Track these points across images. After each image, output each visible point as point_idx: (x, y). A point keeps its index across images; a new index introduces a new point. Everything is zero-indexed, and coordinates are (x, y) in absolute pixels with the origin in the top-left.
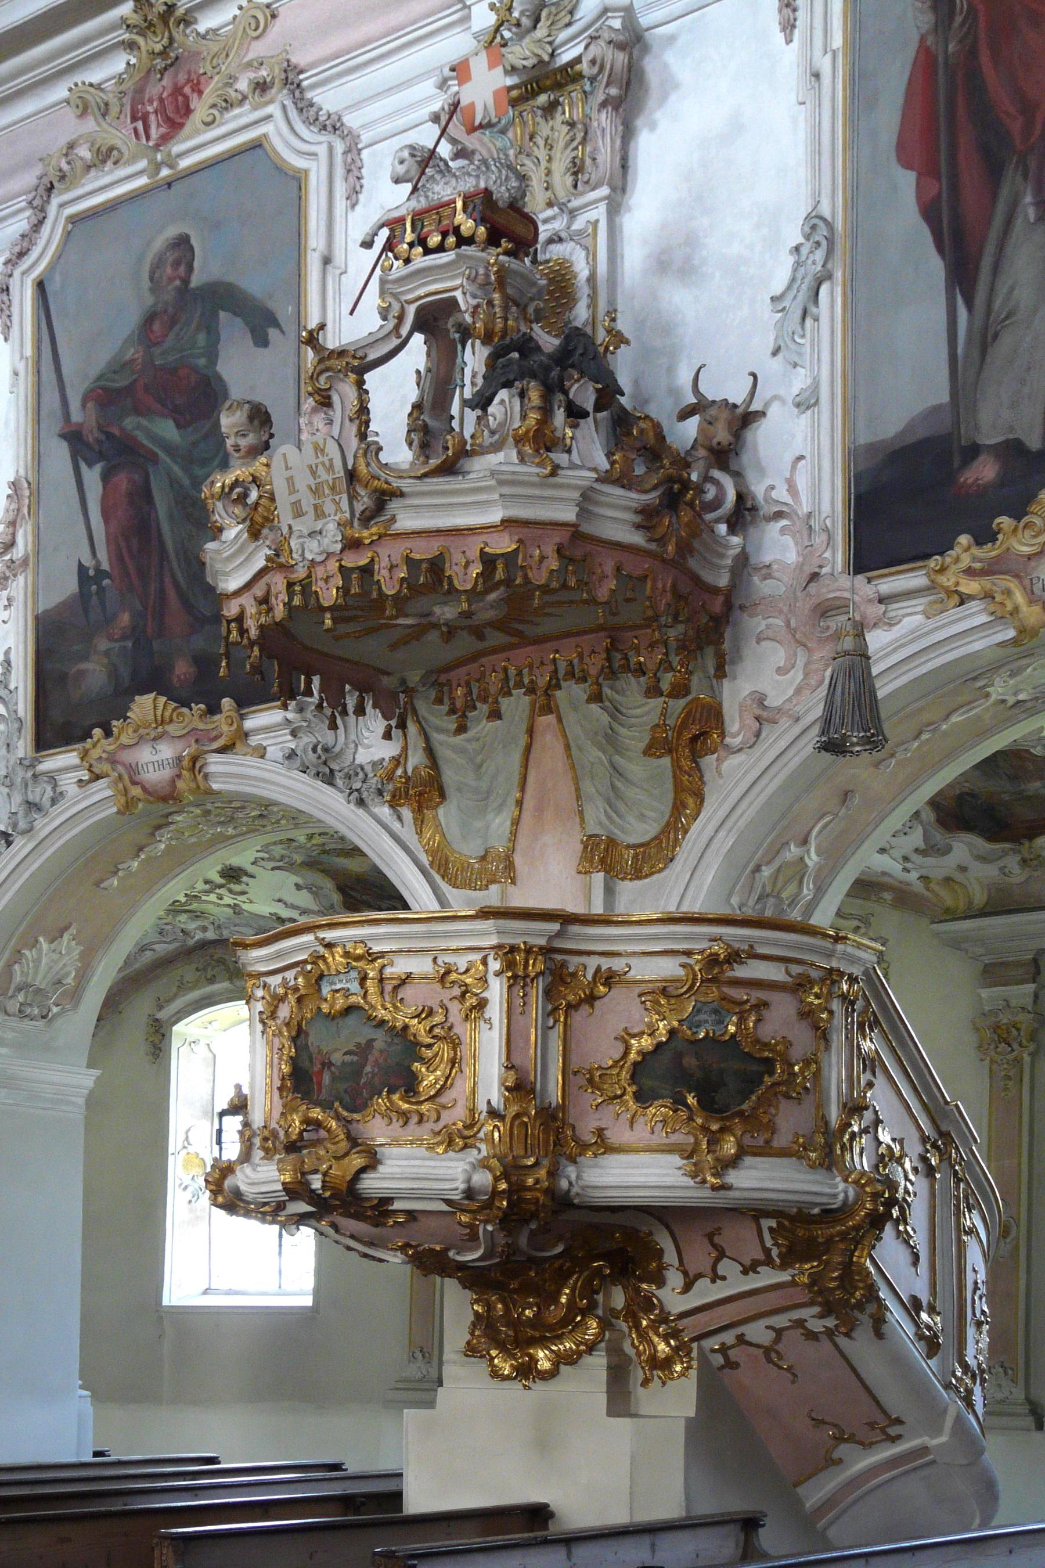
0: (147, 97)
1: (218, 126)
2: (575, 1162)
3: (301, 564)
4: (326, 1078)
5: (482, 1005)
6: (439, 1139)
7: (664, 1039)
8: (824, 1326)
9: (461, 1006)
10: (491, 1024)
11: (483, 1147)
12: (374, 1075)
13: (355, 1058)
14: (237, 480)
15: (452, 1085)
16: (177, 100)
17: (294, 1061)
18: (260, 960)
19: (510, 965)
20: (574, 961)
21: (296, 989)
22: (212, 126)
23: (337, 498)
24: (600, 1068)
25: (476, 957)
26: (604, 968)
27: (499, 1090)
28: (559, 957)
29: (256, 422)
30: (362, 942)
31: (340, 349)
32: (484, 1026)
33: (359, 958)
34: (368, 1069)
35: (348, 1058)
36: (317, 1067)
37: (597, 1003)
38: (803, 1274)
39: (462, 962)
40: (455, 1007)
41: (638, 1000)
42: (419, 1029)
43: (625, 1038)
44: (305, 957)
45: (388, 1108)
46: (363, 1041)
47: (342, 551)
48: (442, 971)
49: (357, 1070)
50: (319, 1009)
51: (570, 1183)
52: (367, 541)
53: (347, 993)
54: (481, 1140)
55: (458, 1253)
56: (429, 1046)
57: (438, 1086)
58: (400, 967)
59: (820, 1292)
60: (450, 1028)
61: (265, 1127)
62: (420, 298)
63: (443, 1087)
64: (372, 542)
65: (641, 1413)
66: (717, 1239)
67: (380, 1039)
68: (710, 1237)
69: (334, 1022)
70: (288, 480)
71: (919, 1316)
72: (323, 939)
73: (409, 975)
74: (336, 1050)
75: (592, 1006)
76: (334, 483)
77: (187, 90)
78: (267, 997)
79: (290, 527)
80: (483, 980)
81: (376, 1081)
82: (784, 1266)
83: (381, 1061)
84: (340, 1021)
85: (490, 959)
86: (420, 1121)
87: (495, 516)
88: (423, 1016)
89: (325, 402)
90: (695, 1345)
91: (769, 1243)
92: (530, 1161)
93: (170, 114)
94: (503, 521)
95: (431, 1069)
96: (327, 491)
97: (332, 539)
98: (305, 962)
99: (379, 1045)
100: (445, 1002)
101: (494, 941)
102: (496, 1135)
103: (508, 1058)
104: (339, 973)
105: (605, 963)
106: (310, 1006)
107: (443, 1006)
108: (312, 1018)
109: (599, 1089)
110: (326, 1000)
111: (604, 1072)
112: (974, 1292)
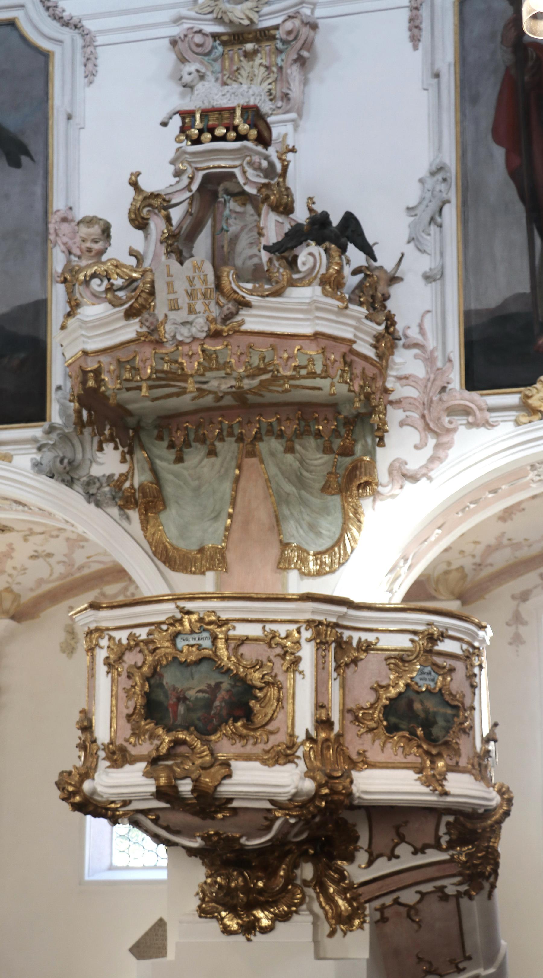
3: (171, 342)
4: (181, 709)
5: (297, 661)
7: (403, 691)
9: (282, 662)
10: (304, 675)
12: (221, 706)
13: (206, 695)
14: (95, 272)
15: (276, 717)
17: (147, 696)
19: (318, 634)
20: (346, 634)
24: (362, 708)
25: (293, 627)
26: (363, 639)
28: (340, 631)
30: (214, 612)
31: (156, 193)
32: (298, 677)
34: (217, 703)
35: (200, 695)
36: (172, 701)
37: (360, 664)
39: (282, 630)
40: (278, 661)
41: (384, 663)
42: (256, 677)
43: (377, 688)
45: (233, 733)
46: (213, 683)
47: (205, 338)
49: (208, 704)
52: (225, 334)
55: (247, 840)
56: (261, 689)
58: (242, 630)
60: (276, 676)
61: (111, 743)
62: (209, 168)
65: (329, 956)
66: (402, 830)
68: (397, 828)
69: (189, 669)
72: (183, 608)
74: (190, 689)
75: (356, 665)
79: (166, 316)
80: (298, 643)
81: (224, 712)
84: (194, 669)
85: (303, 630)
86: (255, 743)
87: (308, 330)
88: (258, 667)
90: (367, 905)
96: (199, 296)
100: (272, 658)
101: (309, 616)
105: (365, 636)
108: (167, 665)
109: (362, 723)
111: (366, 711)
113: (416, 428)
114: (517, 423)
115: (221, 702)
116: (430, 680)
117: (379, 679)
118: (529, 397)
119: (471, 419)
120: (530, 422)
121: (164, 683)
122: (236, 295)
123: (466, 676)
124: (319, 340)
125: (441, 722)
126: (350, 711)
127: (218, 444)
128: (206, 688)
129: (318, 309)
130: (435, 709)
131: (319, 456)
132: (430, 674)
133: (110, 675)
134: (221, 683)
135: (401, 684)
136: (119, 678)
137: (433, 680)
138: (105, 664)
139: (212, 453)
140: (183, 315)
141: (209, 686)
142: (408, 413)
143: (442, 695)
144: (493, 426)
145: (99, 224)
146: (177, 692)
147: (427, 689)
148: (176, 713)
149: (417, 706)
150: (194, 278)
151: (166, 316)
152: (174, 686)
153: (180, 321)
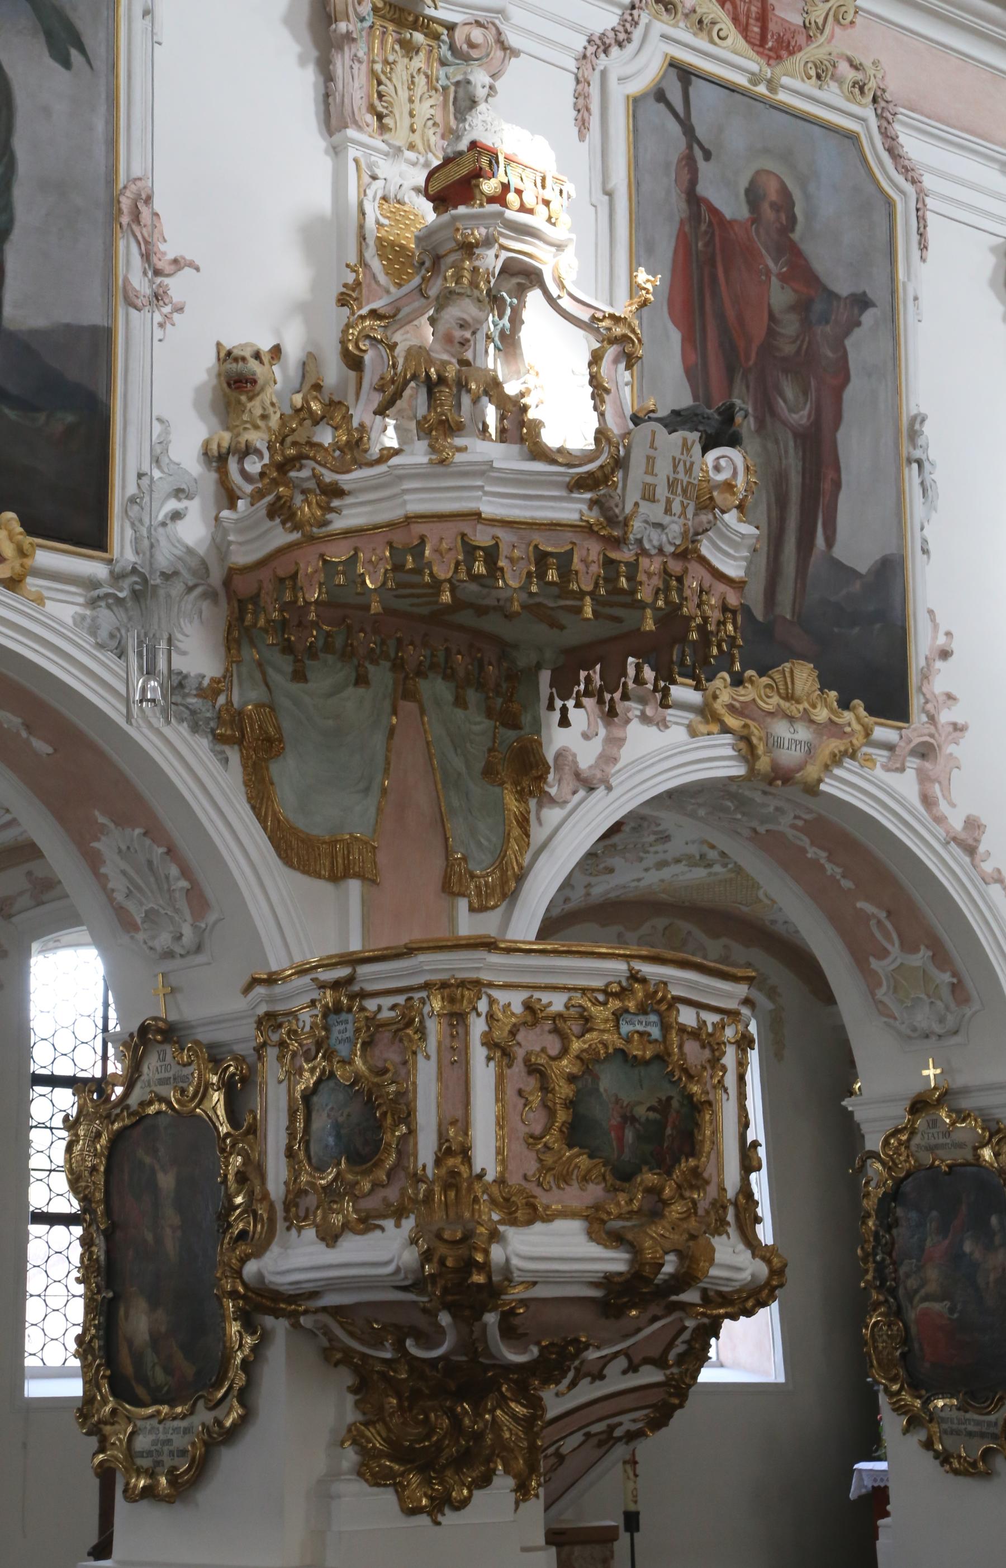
34: (669, 1131)
35: (652, 1115)
46: (664, 1098)
74: (640, 1103)
99: (675, 1104)
114: (693, 733)
121: (602, 1090)
127: (371, 668)
128: (656, 1104)
131: (478, 719)
133: (492, 1064)
136: (509, 1071)
138: (483, 1044)
139: (361, 680)
140: (655, 512)
141: (660, 1101)
146: (622, 1107)
148: (621, 1139)
151: (636, 504)
152: (616, 1096)
153: (653, 519)
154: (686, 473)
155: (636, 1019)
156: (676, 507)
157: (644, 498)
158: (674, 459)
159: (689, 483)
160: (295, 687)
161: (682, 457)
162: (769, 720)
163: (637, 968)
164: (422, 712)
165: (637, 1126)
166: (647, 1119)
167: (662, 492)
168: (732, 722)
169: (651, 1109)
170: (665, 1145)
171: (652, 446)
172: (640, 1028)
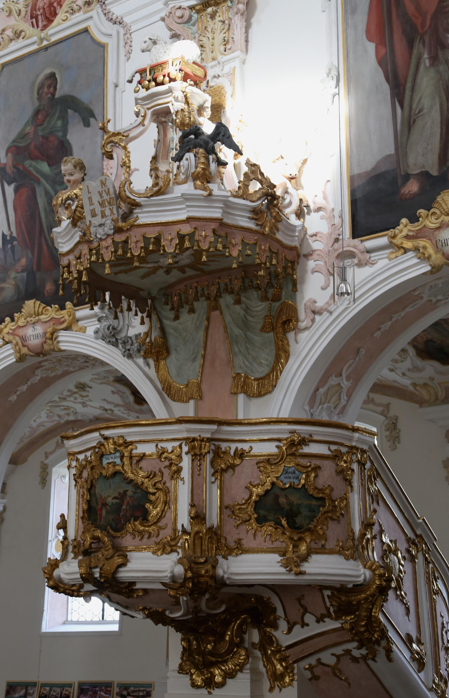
0: (37, 7)
1: (69, 21)
2: (227, 559)
6: (159, 546)
8: (361, 654)
11: (180, 551)
12: (126, 509)
16: (50, 9)
18: (73, 446)
21: (90, 462)
22: (66, 21)
23: (111, 207)
27: (188, 518)
29: (78, 168)
33: (120, 445)
38: (347, 623)
44: (95, 444)
48: (160, 453)
50: (101, 473)
51: (224, 572)
53: (114, 464)
54: (179, 547)
56: (154, 494)
57: (158, 517)
59: (356, 634)
60: (164, 484)
63: (160, 516)
64: (127, 229)
67: (130, 490)
70: (89, 198)
71: (412, 646)
73: (144, 455)
76: (110, 200)
77: (55, 4)
78: (78, 466)
82: (337, 618)
83: (130, 502)
87: (183, 217)
89: (111, 157)
91: (328, 604)
92: (202, 560)
93: (48, 16)
94: (187, 218)
95: (155, 506)
97: (108, 229)
98: (94, 447)
102: (186, 545)
103: (192, 500)
104: (111, 453)
106: (97, 472)
107: (160, 471)
110: (104, 468)
112: (442, 630)
113: (322, 273)
115: (127, 506)
116: (293, 478)
117: (252, 480)
118: (394, 237)
119: (356, 261)
120: (396, 257)
122: (129, 199)
123: (336, 471)
124: (190, 222)
125: (305, 512)
126: (227, 507)
128: (118, 495)
129: (187, 199)
130: (299, 502)
132: (294, 473)
134: (127, 491)
135: (268, 483)
137: (297, 478)
140: (97, 221)
142: (317, 262)
143: (306, 490)
144: (373, 264)
145: (71, 162)
147: (290, 486)
149: (282, 500)
150: (102, 192)
154: (107, 194)
155: (110, 457)
156: (108, 212)
157: (92, 217)
158: (99, 192)
159: (110, 198)
160: (175, 324)
161: (103, 189)
162: (436, 233)
163: (103, 433)
164: (221, 313)
165: (107, 507)
166: (112, 503)
167: (98, 209)
168: (408, 244)
169: (115, 498)
170: (121, 514)
171: (89, 193)
172: (111, 460)
